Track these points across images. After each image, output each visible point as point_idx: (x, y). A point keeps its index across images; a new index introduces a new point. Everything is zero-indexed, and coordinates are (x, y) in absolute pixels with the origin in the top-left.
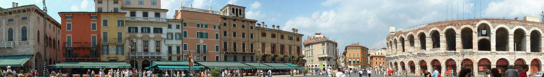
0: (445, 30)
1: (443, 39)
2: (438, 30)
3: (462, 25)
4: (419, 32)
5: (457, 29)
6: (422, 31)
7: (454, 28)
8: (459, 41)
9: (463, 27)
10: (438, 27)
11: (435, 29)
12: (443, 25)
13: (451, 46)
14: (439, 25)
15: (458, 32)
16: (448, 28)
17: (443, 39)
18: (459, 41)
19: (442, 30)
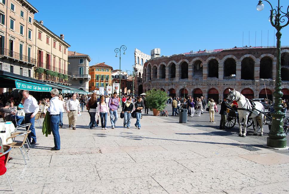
0: (242, 58)
1: (239, 67)
2: (234, 58)
3: (262, 54)
4: (210, 59)
5: (257, 58)
6: (214, 58)
7: (253, 57)
8: (257, 70)
9: (262, 56)
10: (235, 55)
11: (230, 56)
12: (241, 52)
13: (184, 75)
14: (236, 53)
15: (257, 61)
16: (246, 56)
17: (239, 67)
18: (257, 70)
19: (239, 58)
